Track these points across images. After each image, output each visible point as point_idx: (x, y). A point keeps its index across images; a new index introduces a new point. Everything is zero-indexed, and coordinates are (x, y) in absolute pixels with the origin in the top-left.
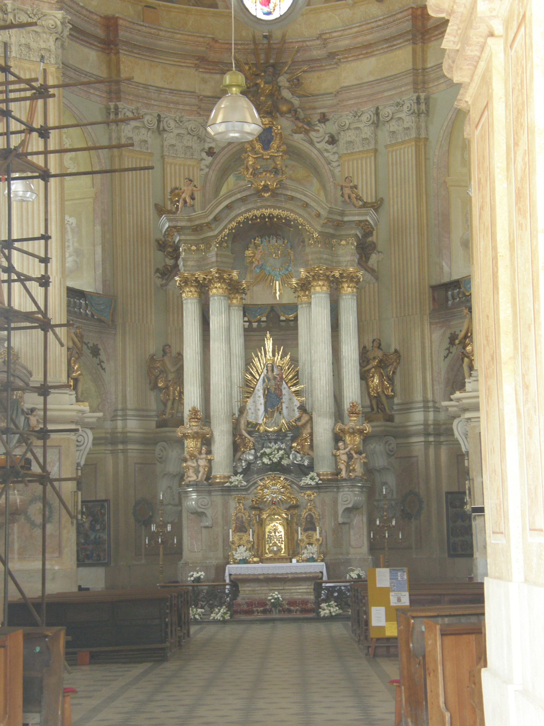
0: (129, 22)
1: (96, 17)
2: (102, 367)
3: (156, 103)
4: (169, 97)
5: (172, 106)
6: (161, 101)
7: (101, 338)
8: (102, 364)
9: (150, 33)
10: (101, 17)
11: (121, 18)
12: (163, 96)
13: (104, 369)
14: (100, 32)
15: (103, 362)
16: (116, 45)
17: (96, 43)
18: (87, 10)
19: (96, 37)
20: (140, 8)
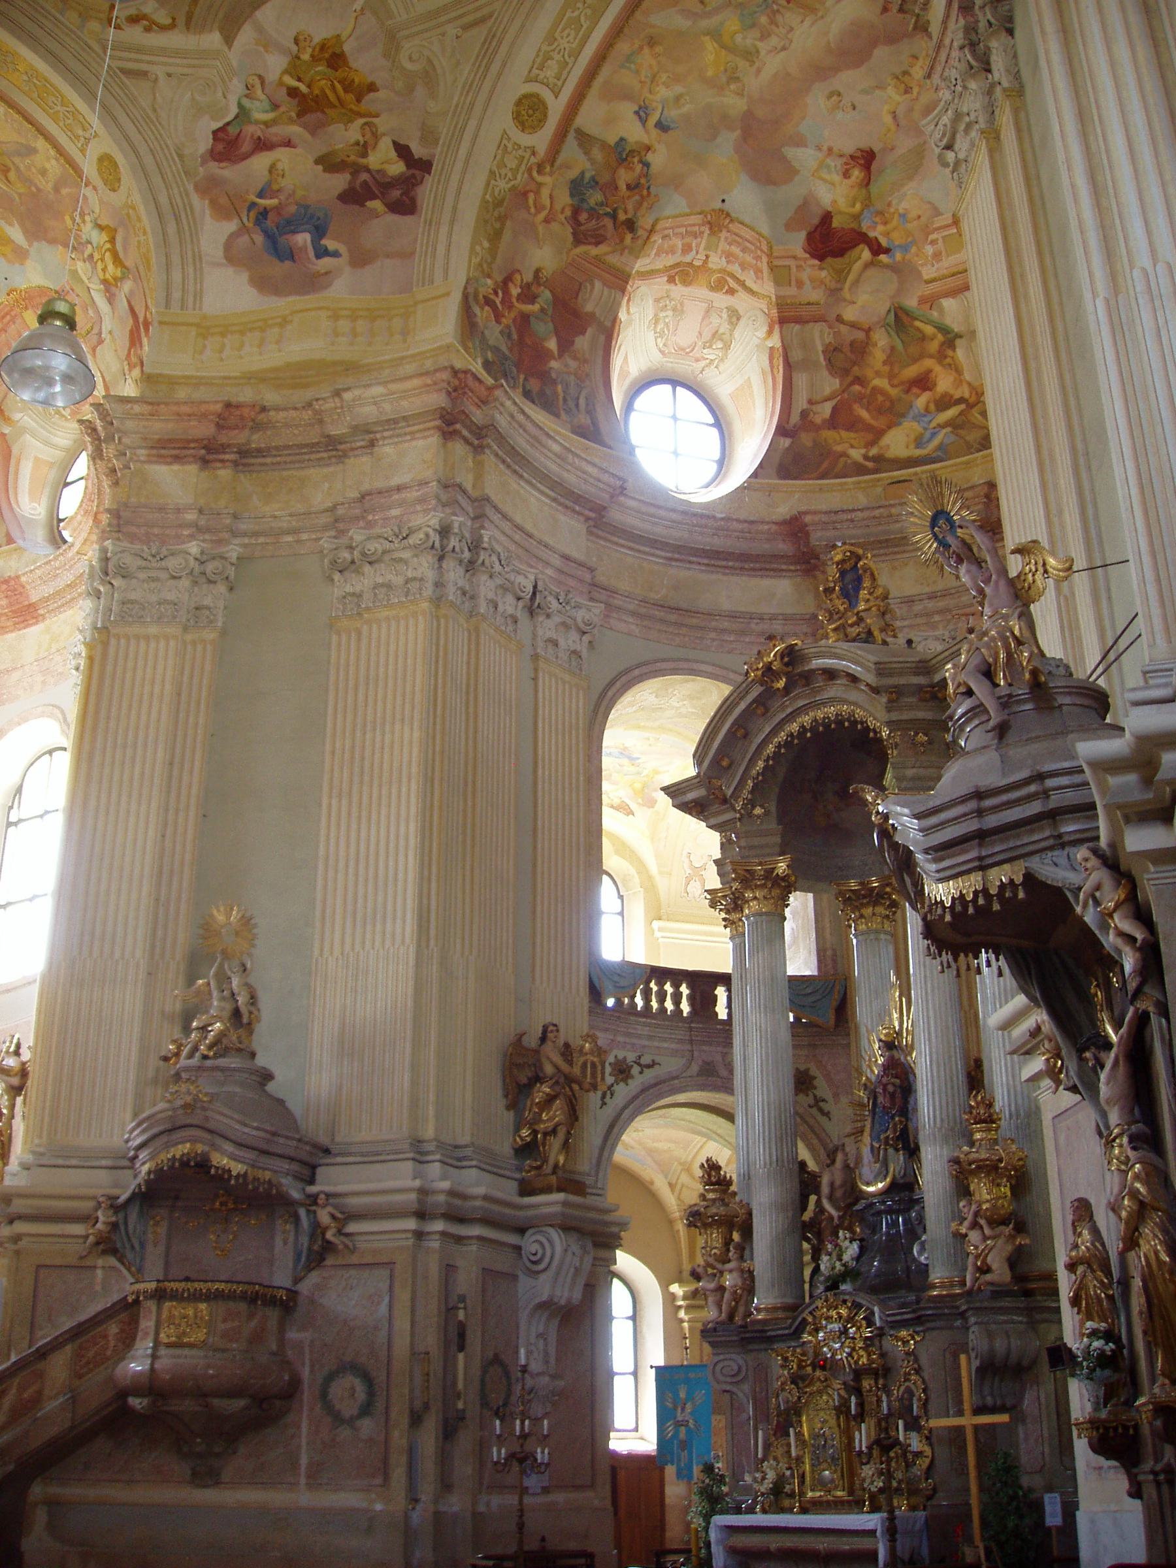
0: (826, 513)
1: (766, 527)
2: (821, 1111)
3: (906, 623)
4: (930, 605)
5: (937, 618)
6: (916, 616)
7: (814, 1056)
8: (821, 1104)
9: (874, 517)
10: (776, 523)
11: (806, 513)
12: (918, 608)
13: (827, 1114)
14: (784, 547)
15: (823, 1100)
16: (817, 558)
17: (784, 567)
18: (738, 521)
19: (776, 557)
20: (879, 490)
